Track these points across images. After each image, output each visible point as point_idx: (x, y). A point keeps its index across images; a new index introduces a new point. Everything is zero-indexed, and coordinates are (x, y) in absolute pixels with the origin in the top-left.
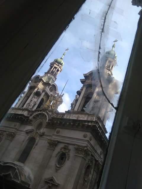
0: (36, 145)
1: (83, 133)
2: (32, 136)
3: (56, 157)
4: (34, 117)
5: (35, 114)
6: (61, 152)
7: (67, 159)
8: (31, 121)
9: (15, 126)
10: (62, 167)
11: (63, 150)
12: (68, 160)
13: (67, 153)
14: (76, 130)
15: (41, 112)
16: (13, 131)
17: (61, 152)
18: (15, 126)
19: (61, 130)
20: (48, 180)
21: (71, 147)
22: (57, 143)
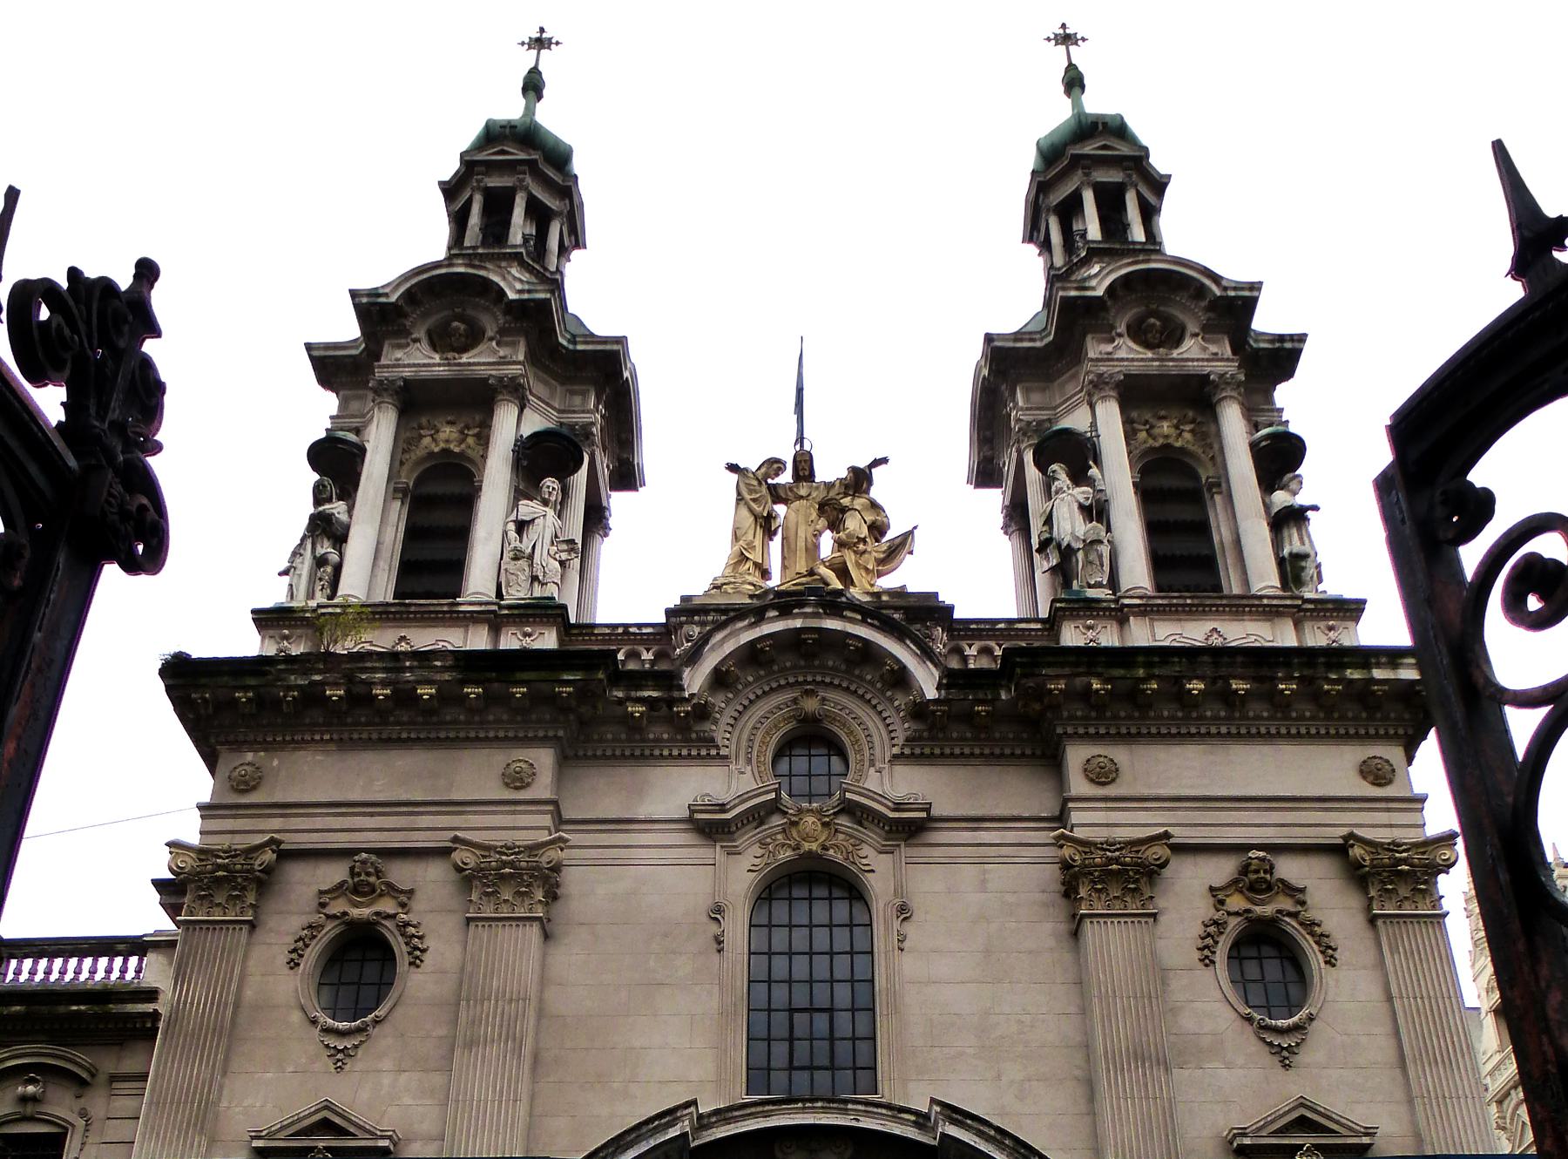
0: (904, 912)
1: (1353, 754)
2: (786, 855)
3: (1208, 962)
4: (720, 679)
5: (729, 647)
6: (1233, 922)
7: (1315, 959)
8: (703, 712)
9: (517, 780)
10: (1311, 1018)
11: (1236, 902)
12: (1331, 962)
13: (1294, 915)
14: (1269, 737)
15: (798, 623)
16: (531, 828)
17: (1233, 922)
18: (517, 780)
19: (1120, 754)
20: (1270, 1135)
21: (1289, 869)
22: (1160, 851)
